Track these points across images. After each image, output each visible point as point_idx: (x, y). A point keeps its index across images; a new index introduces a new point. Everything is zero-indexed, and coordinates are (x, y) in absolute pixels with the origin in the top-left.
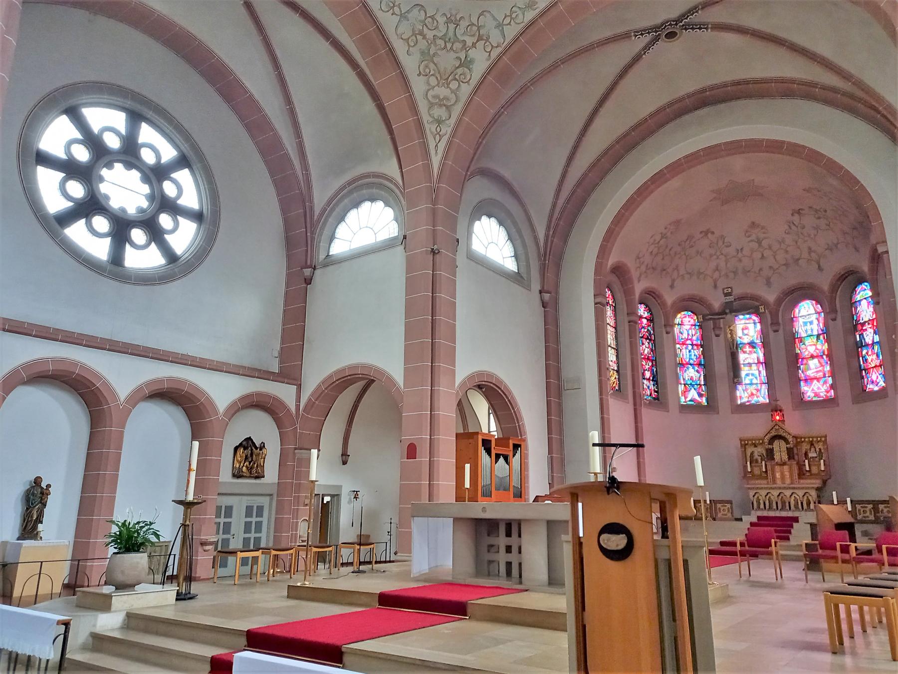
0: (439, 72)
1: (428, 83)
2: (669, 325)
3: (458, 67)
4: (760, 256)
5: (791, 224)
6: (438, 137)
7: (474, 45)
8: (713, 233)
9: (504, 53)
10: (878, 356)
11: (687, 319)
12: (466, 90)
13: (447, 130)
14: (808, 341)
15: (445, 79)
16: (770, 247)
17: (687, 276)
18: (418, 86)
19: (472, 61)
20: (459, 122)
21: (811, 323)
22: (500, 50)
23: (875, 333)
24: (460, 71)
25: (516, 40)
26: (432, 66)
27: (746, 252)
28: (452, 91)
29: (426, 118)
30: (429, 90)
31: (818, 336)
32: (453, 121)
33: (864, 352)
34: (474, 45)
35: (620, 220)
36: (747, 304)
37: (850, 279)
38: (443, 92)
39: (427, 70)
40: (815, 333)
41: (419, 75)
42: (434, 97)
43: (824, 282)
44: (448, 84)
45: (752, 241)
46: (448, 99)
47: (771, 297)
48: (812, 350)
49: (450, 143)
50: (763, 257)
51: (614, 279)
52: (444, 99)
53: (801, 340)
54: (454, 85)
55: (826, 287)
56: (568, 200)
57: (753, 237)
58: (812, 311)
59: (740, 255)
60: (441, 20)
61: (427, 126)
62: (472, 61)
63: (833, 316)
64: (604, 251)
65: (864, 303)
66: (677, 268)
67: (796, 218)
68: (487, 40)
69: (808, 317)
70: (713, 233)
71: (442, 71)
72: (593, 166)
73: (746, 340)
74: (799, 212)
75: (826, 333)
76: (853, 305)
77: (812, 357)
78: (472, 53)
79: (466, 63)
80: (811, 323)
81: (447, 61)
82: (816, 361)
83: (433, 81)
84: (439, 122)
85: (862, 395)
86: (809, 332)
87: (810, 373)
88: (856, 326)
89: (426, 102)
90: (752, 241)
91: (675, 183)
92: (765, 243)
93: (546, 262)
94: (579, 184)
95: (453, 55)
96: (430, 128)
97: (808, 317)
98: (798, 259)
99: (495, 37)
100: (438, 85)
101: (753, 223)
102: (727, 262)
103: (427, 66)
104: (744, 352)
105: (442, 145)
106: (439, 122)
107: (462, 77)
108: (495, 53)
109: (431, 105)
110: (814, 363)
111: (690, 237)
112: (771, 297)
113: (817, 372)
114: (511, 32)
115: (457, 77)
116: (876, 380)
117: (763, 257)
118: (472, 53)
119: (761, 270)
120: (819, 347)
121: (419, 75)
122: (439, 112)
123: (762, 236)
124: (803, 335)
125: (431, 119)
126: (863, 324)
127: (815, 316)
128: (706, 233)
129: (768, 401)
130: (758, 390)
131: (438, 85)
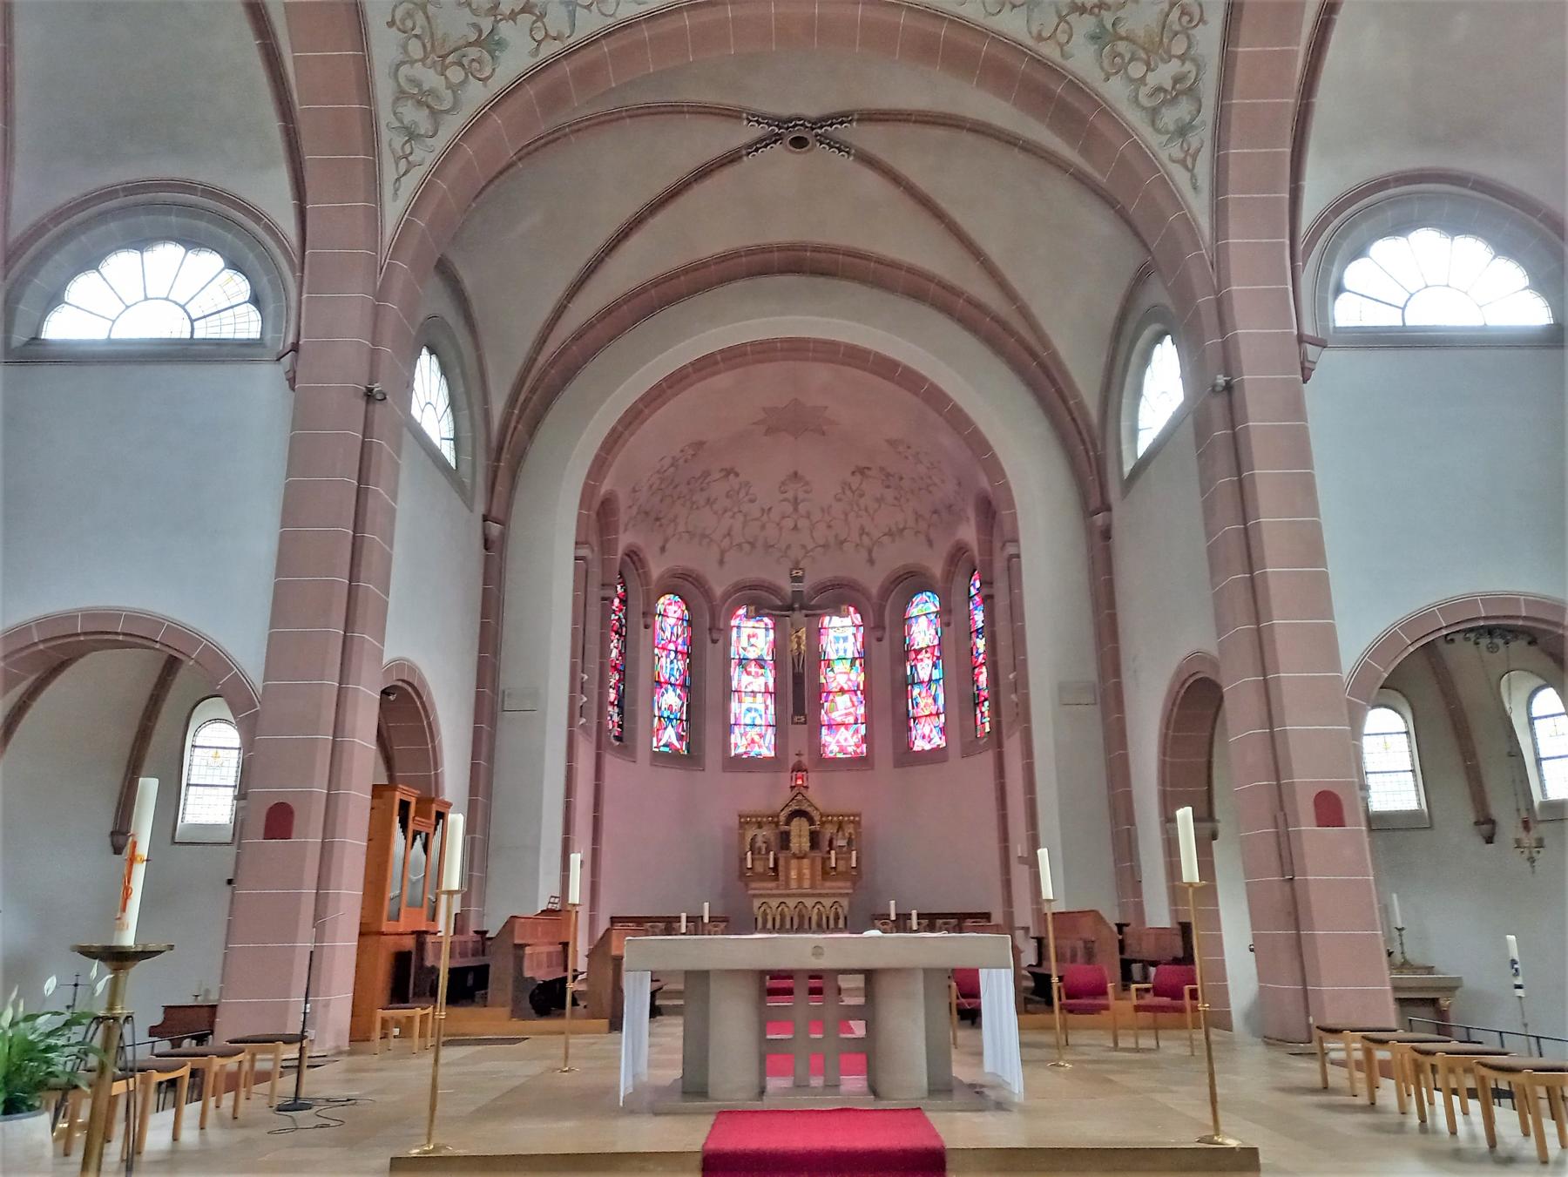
0: (432, 35)
1: (405, 48)
2: (649, 613)
3: (470, 44)
4: (791, 525)
5: (846, 485)
6: (403, 164)
7: (513, 16)
8: (737, 475)
9: (569, 53)
10: (935, 700)
11: (674, 608)
12: (477, 95)
13: (426, 155)
15: (442, 55)
16: (808, 516)
17: (686, 536)
18: (384, 47)
19: (501, 44)
20: (453, 150)
21: (845, 639)
22: (557, 46)
23: (935, 665)
24: (473, 52)
25: (592, 42)
26: (420, 19)
27: (775, 515)
29: (385, 116)
30: (403, 63)
31: (853, 660)
33: (916, 691)
34: (513, 16)
35: (634, 417)
36: (838, 595)
37: (910, 582)
38: (431, 79)
39: (409, 24)
40: (849, 655)
41: (391, 24)
42: (412, 81)
43: (873, 581)
44: (445, 68)
45: (785, 500)
46: (438, 98)
48: (842, 681)
49: (427, 188)
50: (795, 528)
51: (600, 516)
52: (431, 92)
53: (829, 663)
54: (456, 75)
56: (552, 363)
57: (790, 495)
59: (765, 518)
61: (385, 135)
62: (501, 44)
63: (879, 634)
64: (599, 466)
65: (923, 620)
66: (674, 520)
67: (855, 481)
68: (541, 17)
70: (737, 475)
71: (439, 34)
72: (609, 311)
73: (752, 654)
74: (861, 471)
75: (865, 659)
77: (842, 691)
78: (505, 29)
79: (491, 43)
80: (845, 639)
82: (846, 697)
83: (415, 49)
84: (412, 135)
85: (907, 757)
86: (841, 654)
87: (837, 716)
88: (905, 653)
89: (391, 82)
90: (785, 500)
91: (723, 381)
92: (801, 507)
93: (502, 455)
94: (579, 336)
95: (467, 16)
96: (390, 140)
98: (842, 543)
99: (556, 19)
100: (423, 60)
101: (796, 474)
102: (745, 524)
103: (409, 15)
104: (749, 673)
105: (411, 183)
107: (475, 65)
108: (550, 49)
109: (401, 95)
110: (843, 701)
111: (706, 474)
113: (847, 715)
115: (465, 61)
116: (927, 736)
117: (795, 528)
118: (505, 29)
119: (789, 547)
120: (853, 676)
121: (391, 24)
123: (801, 495)
124: (833, 656)
125: (397, 124)
126: (918, 652)
127: (853, 630)
128: (729, 472)
129: (772, 754)
130: (761, 736)
131: (423, 60)
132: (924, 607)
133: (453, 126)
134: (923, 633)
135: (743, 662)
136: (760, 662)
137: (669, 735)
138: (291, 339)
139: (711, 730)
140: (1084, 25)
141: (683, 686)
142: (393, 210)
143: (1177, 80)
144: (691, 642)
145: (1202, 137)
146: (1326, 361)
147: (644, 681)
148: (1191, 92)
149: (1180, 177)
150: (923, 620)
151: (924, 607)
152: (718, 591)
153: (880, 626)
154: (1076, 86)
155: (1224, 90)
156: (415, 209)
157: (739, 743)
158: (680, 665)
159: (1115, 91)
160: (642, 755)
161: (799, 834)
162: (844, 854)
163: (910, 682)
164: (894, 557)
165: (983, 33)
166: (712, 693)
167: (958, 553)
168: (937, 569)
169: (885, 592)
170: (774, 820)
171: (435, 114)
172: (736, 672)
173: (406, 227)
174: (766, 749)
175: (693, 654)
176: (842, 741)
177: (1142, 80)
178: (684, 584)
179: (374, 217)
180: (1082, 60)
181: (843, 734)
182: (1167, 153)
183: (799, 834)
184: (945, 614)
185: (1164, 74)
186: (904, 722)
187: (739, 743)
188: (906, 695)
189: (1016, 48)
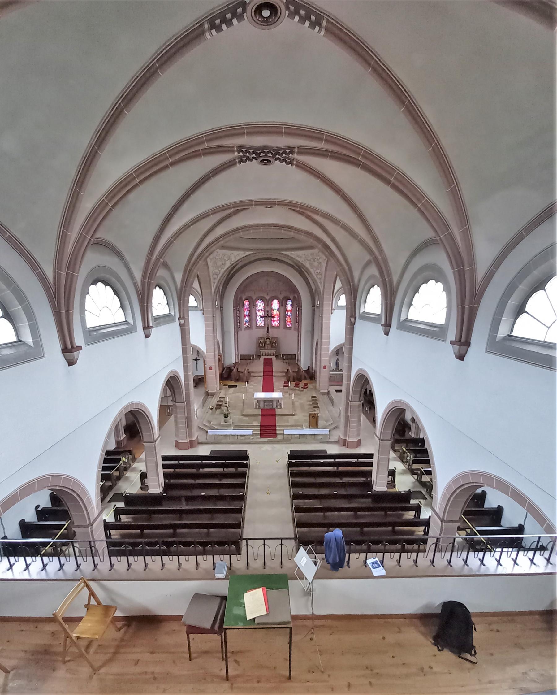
12: (223, 271)
13: (217, 281)
14: (275, 311)
18: (211, 269)
20: (220, 279)
29: (211, 277)
32: (218, 279)
37: (287, 299)
38: (217, 271)
43: (281, 297)
47: (268, 298)
49: (217, 285)
55: (281, 299)
60: (221, 255)
69: (275, 304)
75: (279, 310)
76: (287, 304)
78: (226, 262)
81: (219, 263)
84: (215, 279)
88: (286, 310)
96: (212, 280)
97: (275, 304)
106: (215, 279)
112: (268, 298)
114: (238, 258)
116: (289, 325)
118: (226, 262)
122: (215, 276)
132: (290, 302)
134: (289, 307)
135: (259, 310)
136: (261, 310)
137: (247, 324)
139: (254, 322)
140: (308, 262)
141: (249, 316)
144: (249, 308)
145: (322, 280)
146: (335, 312)
147: (243, 316)
148: (321, 274)
149: (319, 284)
151: (290, 302)
152: (254, 299)
153: (282, 305)
154: (307, 268)
155: (325, 277)
156: (216, 287)
157: (258, 324)
158: (248, 312)
159: (312, 271)
160: (243, 329)
161: (268, 341)
162: (275, 344)
163: (287, 315)
165: (294, 259)
166: (254, 316)
167: (294, 297)
168: (292, 298)
169: (283, 299)
170: (264, 338)
171: (217, 275)
172: (257, 312)
173: (215, 292)
174: (262, 325)
175: (250, 311)
176: (275, 324)
178: (249, 299)
180: (308, 266)
181: (275, 322)
182: (318, 281)
183: (268, 341)
184: (292, 305)
185: (318, 271)
186: (285, 322)
187: (258, 324)
189: (299, 262)
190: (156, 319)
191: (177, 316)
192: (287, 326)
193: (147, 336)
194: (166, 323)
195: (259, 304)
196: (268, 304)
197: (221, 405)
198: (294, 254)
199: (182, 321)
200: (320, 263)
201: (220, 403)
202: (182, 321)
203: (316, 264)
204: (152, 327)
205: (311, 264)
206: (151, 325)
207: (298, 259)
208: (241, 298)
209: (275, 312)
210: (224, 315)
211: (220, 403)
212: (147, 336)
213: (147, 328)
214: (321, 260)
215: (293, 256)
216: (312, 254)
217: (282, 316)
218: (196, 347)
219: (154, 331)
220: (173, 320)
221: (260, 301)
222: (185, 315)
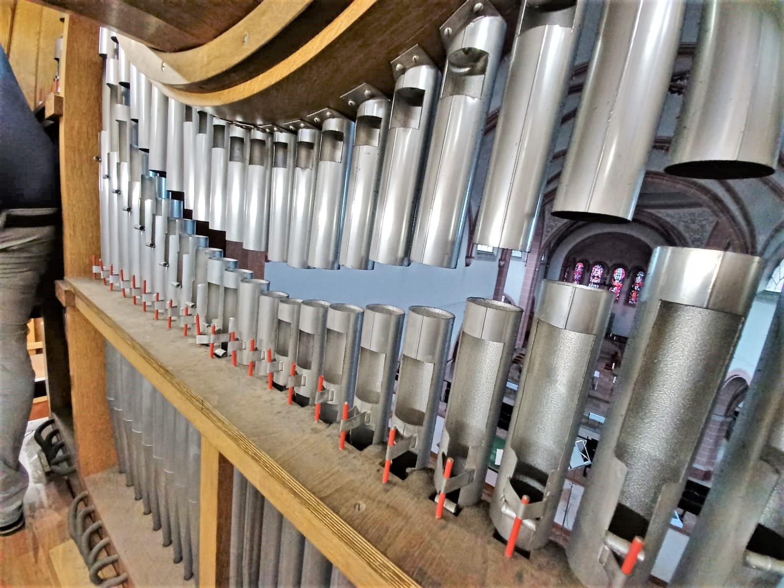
13: (549, 234)
14: (616, 281)
20: (554, 233)
28: (556, 224)
29: (545, 229)
47: (610, 264)
53: (615, 280)
55: (630, 268)
58: (621, 272)
65: (639, 277)
69: (619, 273)
75: (622, 281)
84: (548, 232)
96: (545, 233)
97: (619, 273)
105: (547, 238)
106: (548, 232)
109: (548, 227)
112: (610, 264)
122: (549, 229)
133: (554, 229)
135: (594, 277)
136: (598, 277)
138: (525, 260)
141: (579, 281)
142: (543, 242)
143: (699, 238)
150: (639, 277)
152: (591, 262)
158: (580, 276)
159: (687, 235)
164: (635, 263)
165: (660, 218)
169: (633, 269)
173: (545, 244)
177: (692, 236)
179: (540, 244)
185: (697, 236)
188: (631, 291)
190: (480, 253)
191: (499, 257)
192: (630, 302)
193: (467, 265)
194: (486, 259)
195: (596, 270)
196: (609, 271)
197: (520, 361)
198: (662, 213)
199: (502, 263)
200: (702, 227)
201: (520, 359)
202: (502, 263)
203: (694, 226)
204: (474, 258)
205: (687, 227)
206: (473, 255)
207: (668, 219)
208: (574, 259)
209: (616, 283)
210: (550, 270)
211: (520, 359)
212: (467, 265)
213: (469, 256)
214: (704, 223)
215: (659, 215)
216: (693, 214)
217: (625, 289)
218: (509, 297)
219: (474, 262)
220: (494, 260)
221: (598, 266)
222: (507, 258)
